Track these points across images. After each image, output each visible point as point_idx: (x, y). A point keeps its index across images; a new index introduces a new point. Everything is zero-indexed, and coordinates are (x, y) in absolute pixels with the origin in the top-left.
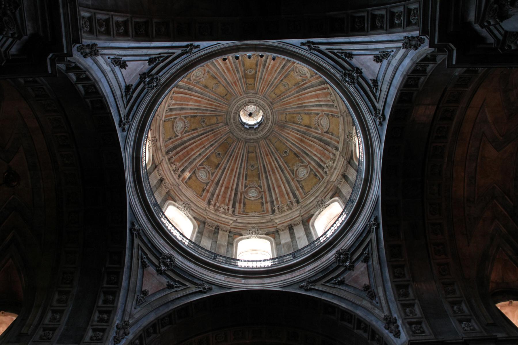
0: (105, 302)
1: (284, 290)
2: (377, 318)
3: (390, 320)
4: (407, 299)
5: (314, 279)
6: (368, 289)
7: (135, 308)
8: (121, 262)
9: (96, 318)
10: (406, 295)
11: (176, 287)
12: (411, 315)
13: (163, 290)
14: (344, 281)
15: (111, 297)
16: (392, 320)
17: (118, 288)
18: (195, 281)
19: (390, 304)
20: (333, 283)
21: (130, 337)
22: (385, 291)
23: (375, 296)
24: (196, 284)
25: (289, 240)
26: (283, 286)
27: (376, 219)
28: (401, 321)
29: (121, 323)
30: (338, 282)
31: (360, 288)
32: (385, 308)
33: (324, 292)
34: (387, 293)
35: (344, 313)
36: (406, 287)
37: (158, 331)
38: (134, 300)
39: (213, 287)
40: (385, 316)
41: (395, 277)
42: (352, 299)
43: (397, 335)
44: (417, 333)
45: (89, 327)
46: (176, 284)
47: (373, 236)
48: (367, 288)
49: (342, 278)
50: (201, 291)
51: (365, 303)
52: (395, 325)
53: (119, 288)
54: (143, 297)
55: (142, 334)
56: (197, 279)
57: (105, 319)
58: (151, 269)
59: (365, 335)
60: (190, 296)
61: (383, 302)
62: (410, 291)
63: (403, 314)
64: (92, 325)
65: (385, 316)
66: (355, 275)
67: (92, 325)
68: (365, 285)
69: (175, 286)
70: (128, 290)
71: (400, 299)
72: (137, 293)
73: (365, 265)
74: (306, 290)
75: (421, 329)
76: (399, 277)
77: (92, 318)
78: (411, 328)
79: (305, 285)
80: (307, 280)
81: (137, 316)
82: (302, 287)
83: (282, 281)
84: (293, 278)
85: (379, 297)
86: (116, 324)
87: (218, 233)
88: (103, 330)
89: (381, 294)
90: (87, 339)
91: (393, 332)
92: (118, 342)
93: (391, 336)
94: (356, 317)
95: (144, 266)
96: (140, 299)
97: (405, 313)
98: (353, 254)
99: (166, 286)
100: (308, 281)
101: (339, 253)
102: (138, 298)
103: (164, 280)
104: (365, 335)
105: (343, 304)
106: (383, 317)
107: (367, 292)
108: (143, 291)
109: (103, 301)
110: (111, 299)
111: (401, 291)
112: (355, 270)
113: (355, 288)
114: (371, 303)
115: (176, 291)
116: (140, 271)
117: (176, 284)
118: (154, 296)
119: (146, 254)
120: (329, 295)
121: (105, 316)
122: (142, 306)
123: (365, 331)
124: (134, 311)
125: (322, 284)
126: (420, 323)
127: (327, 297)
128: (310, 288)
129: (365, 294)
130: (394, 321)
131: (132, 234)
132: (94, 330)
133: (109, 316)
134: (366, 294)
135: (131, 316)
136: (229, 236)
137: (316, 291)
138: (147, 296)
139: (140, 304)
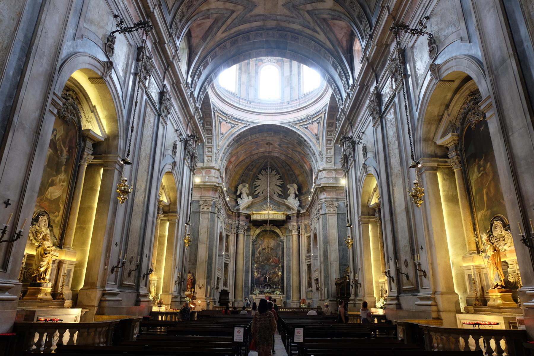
0: (208, 142)
5: (295, 123)
8: (211, 125)
9: (206, 151)
10: (330, 144)
13: (230, 129)
15: (210, 141)
21: (221, 155)
22: (322, 140)
25: (289, 74)
27: (325, 110)
32: (321, 147)
35: (305, 141)
39: (250, 123)
41: (327, 135)
42: (309, 137)
43: (322, 160)
47: (323, 115)
48: (316, 135)
51: (314, 140)
53: (213, 137)
58: (224, 122)
61: (321, 144)
72: (220, 135)
73: (317, 125)
87: (249, 63)
89: (321, 140)
90: (206, 161)
93: (320, 159)
95: (220, 122)
97: (327, 152)
98: (313, 118)
101: (308, 116)
103: (229, 125)
113: (311, 133)
116: (219, 125)
119: (220, 117)
121: (210, 149)
131: (214, 113)
133: (211, 149)
136: (256, 64)
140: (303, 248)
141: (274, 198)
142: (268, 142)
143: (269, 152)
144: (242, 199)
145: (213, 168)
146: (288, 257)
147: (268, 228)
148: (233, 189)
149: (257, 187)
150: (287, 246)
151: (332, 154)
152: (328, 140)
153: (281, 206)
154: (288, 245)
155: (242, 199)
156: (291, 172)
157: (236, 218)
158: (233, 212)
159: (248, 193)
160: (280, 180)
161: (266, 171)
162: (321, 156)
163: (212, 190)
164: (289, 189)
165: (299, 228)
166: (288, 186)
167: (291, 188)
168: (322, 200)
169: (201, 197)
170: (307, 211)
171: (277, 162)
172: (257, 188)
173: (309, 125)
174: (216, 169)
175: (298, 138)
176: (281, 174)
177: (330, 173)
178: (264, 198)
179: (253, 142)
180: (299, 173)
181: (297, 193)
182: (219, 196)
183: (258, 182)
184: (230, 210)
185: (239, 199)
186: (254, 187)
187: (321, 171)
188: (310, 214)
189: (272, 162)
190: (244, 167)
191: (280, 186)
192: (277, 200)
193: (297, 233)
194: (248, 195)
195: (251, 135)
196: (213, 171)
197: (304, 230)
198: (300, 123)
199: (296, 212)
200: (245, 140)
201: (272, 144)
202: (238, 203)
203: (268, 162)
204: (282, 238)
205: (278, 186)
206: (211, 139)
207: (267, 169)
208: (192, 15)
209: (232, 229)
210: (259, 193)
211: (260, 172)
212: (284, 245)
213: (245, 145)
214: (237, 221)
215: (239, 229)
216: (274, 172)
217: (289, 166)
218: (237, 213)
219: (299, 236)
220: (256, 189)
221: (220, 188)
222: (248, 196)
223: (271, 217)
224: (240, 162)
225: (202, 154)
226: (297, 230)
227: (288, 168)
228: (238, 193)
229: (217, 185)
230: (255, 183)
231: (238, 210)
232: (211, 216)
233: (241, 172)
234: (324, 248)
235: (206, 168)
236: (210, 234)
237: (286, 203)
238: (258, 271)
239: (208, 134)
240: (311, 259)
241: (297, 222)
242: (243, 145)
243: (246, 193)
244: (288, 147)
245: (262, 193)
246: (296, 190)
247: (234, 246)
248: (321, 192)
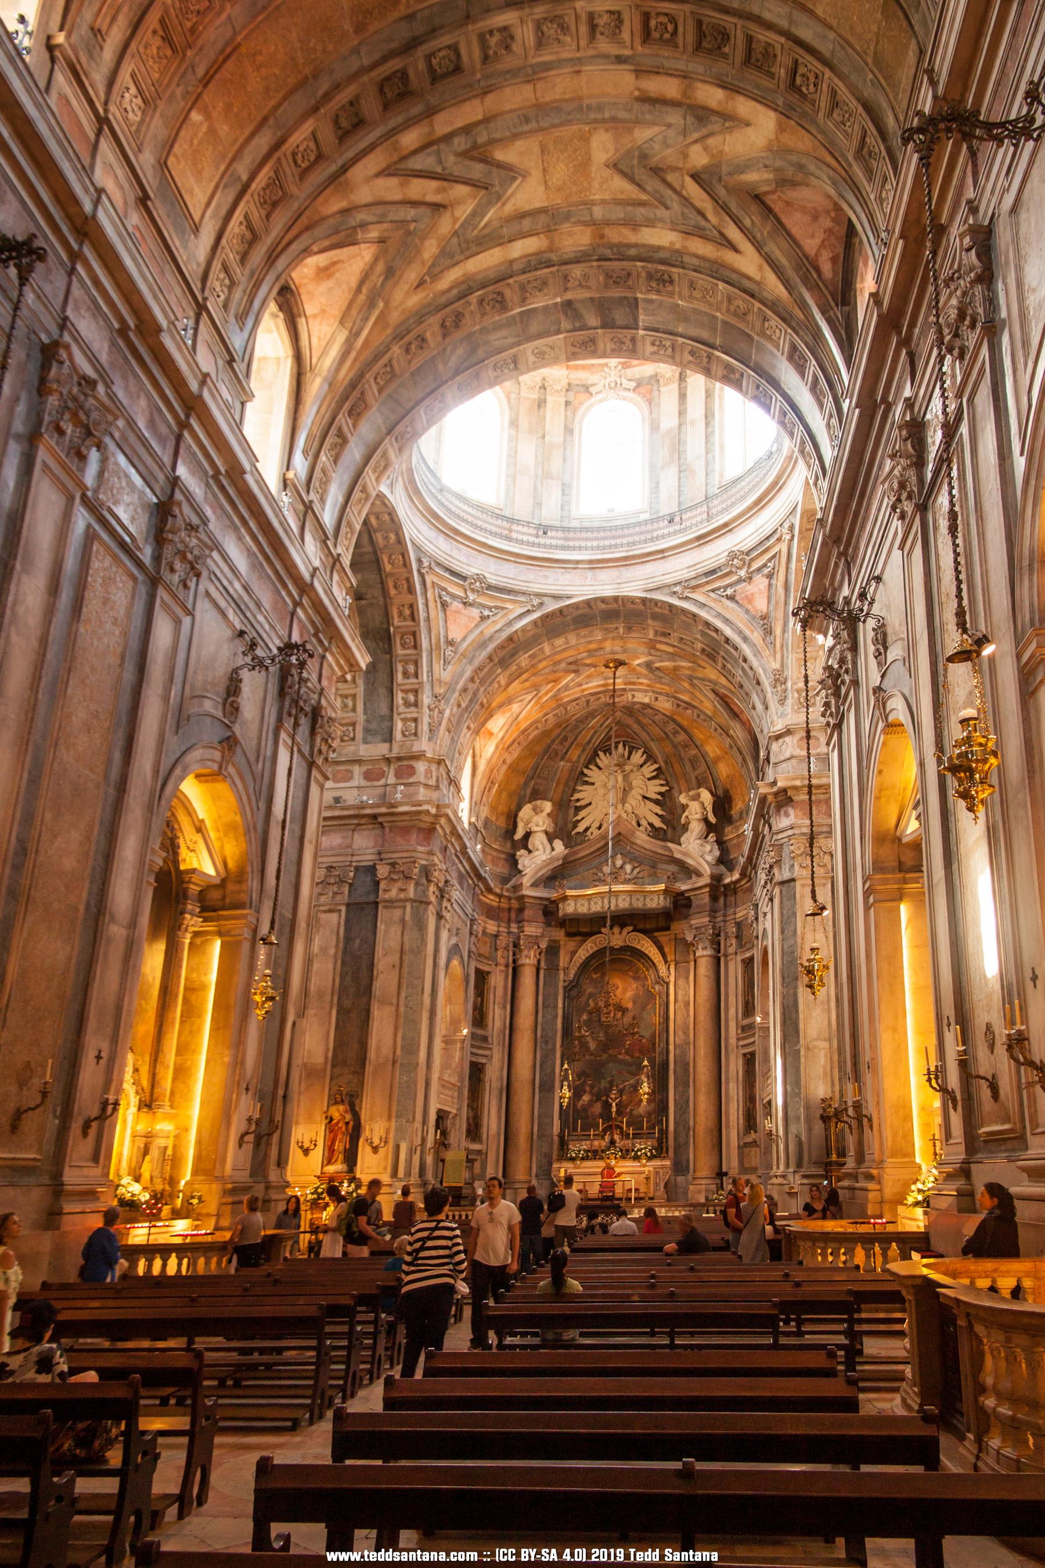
141: (639, 842)
143: (614, 690)
147: (618, 938)
153: (660, 866)
159: (551, 830)
172: (582, 814)
176: (661, 760)
183: (584, 794)
185: (522, 852)
186: (572, 811)
191: (656, 802)
194: (550, 837)
201: (620, 663)
208: (289, 236)
210: (587, 829)
211: (592, 760)
216: (638, 757)
220: (579, 818)
221: (443, 821)
222: (551, 840)
230: (576, 796)
245: (600, 828)
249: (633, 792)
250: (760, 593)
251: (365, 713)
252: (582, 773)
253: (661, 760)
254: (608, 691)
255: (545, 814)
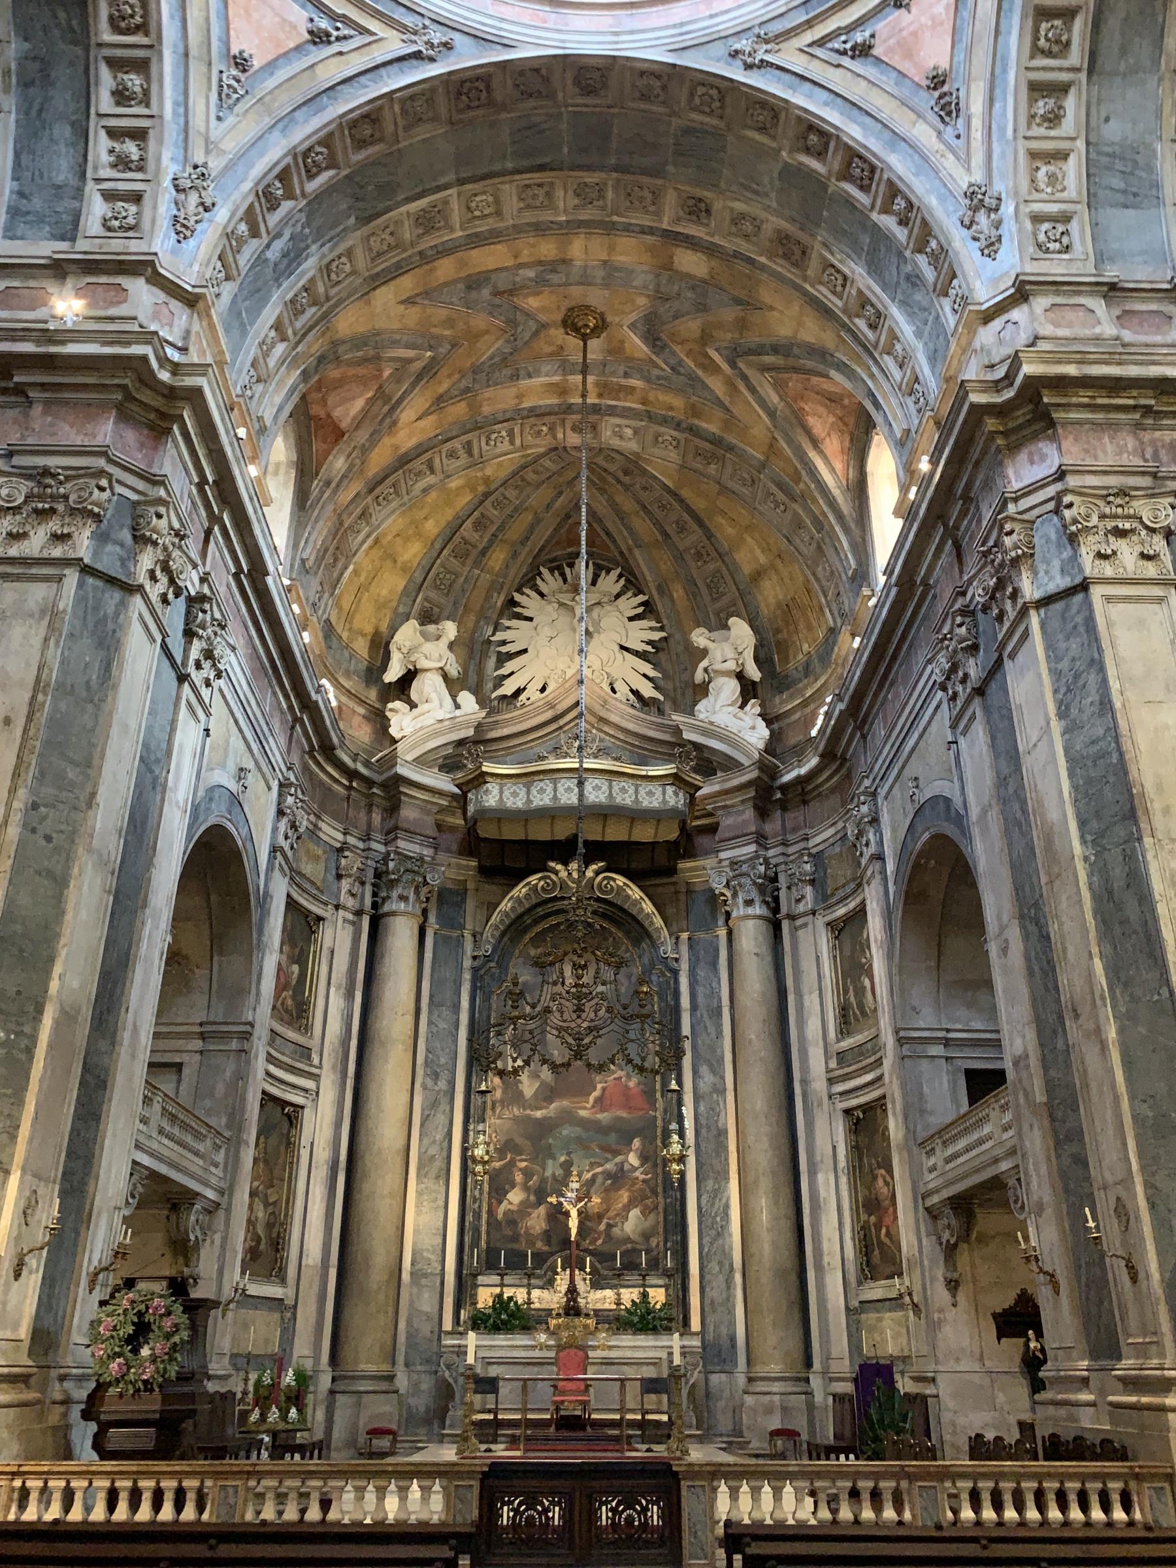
0: (121, 96)
1: (679, 62)
2: (945, 185)
3: (982, 201)
4: (1052, 133)
6: (943, 82)
7: (219, 119)
10: (1054, 119)
11: (338, 39)
12: (1049, 190)
13: (298, 48)
14: (870, 47)
15: (134, 81)
16: (987, 200)
17: (151, 47)
18: (399, 14)
19: (995, 145)
20: (837, 51)
21: (222, 215)
23: (958, 111)
24: (402, 28)
26: (677, 46)
28: (1011, 209)
29: (184, 171)
30: (853, 49)
31: (916, 79)
32: (978, 159)
33: (803, 78)
34: (997, 106)
36: (1062, 89)
37: (298, 192)
38: (210, 89)
39: (457, 36)
40: (970, 185)
43: (990, 248)
44: (1047, 251)
45: (90, 187)
46: (338, 29)
48: (937, 81)
49: (867, 34)
50: (420, 52)
51: (924, 133)
52: (993, 216)
54: (238, 81)
55: (252, 204)
56: (402, 10)
57: (135, 157)
59: (901, 234)
60: (383, 71)
61: (977, 134)
62: (1071, 104)
63: (1024, 184)
64: (98, 180)
65: (970, 185)
66: (911, 28)
67: (98, 180)
68: (935, 68)
69: (335, 33)
70: (186, 55)
71: (1029, 134)
74: (748, 67)
75: (1065, 240)
76: (1049, 54)
77: (90, 158)
78: (1035, 235)
79: (748, 49)
80: (756, 30)
81: (231, 145)
82: (735, 54)
83: (674, 26)
84: (712, 16)
85: (969, 118)
86: (171, 176)
88: (136, 198)
89: (976, 106)
90: (92, 224)
91: (982, 236)
92: (188, 233)
94: (885, 177)
96: (229, 86)
99: (307, 36)
100: (759, 36)
102: (221, 80)
104: (901, 234)
105: (855, 126)
106: (965, 186)
107: (936, 94)
108: (235, 57)
109: (113, 93)
110: (137, 89)
111: (1041, 103)
112: (914, 9)
114: (939, 133)
115: (341, 53)
117: (338, 29)
118: (272, 74)
120: (817, 90)
121: (131, 148)
122: (239, 108)
123: (903, 222)
124: (216, 130)
125: (801, 50)
126: (1066, 218)
127: (809, 96)
128: (762, 61)
129: (925, 101)
130: (994, 202)
132: (110, 196)
134: (933, 103)
135: (209, 146)
137: (778, 72)
138: (251, 71)
139: (231, 102)
140: (811, 1001)
141: (614, 718)
142: (576, 291)
144: (413, 706)
145: (145, 268)
146: (704, 1070)
148: (361, 647)
149: (511, 656)
150: (701, 999)
151: (1072, 192)
152: (1037, 89)
154: (700, 991)
155: (413, 706)
156: (711, 567)
157: (377, 817)
158: (352, 774)
159: (454, 671)
160: (644, 623)
161: (563, 575)
162: (982, 218)
163: (124, 416)
164: (704, 653)
165: (775, 879)
166: (700, 638)
167: (711, 645)
168: (1025, 503)
169: (10, 455)
170: (828, 756)
171: (628, 505)
173: (881, 26)
174: (172, 289)
175: (793, 176)
176: (652, 586)
177: (1069, 315)
178: (549, 715)
179: (474, 282)
180: (763, 559)
181: (754, 673)
182: (208, 533)
183: (516, 634)
184: (328, 749)
185: (397, 704)
186: (492, 662)
187: (988, 317)
188: (848, 776)
189: (602, 509)
190: (432, 527)
192: (631, 726)
193: (758, 909)
194: (453, 685)
195: (461, 182)
196: (139, 289)
197: (809, 890)
198: (809, 24)
199: (754, 774)
200: (427, 222)
202: (394, 731)
203: (578, 507)
204: (667, 948)
205: (637, 654)
206: (142, 66)
207: (571, 565)
209: (345, 884)
210: (519, 692)
211: (530, 581)
212: (677, 994)
213: (426, 294)
214: (377, 836)
215: (392, 884)
216: (610, 583)
217: (700, 523)
218: (384, 786)
219: (776, 927)
220: (504, 671)
222: (454, 697)
223: (597, 793)
224: (404, 461)
225: (74, 182)
226: (761, 889)
227: (695, 536)
228: (393, 674)
229: (164, 376)
230: (499, 636)
231: (391, 760)
232: (80, 600)
233: (413, 552)
234: (1098, 868)
235: (90, 267)
236: (47, 743)
237: (687, 735)
238: (512, 1163)
239: (116, 29)
240: (879, 1062)
241: (761, 839)
242: (407, 284)
243: (445, 676)
244: (706, 338)
245: (543, 690)
246: (749, 656)
247: (349, 995)
248: (1014, 449)
249: (603, 636)
250: (936, 24)
251: (15, 178)
252: (512, 603)
253: (652, 586)
254: (569, 409)
255: (443, 644)
